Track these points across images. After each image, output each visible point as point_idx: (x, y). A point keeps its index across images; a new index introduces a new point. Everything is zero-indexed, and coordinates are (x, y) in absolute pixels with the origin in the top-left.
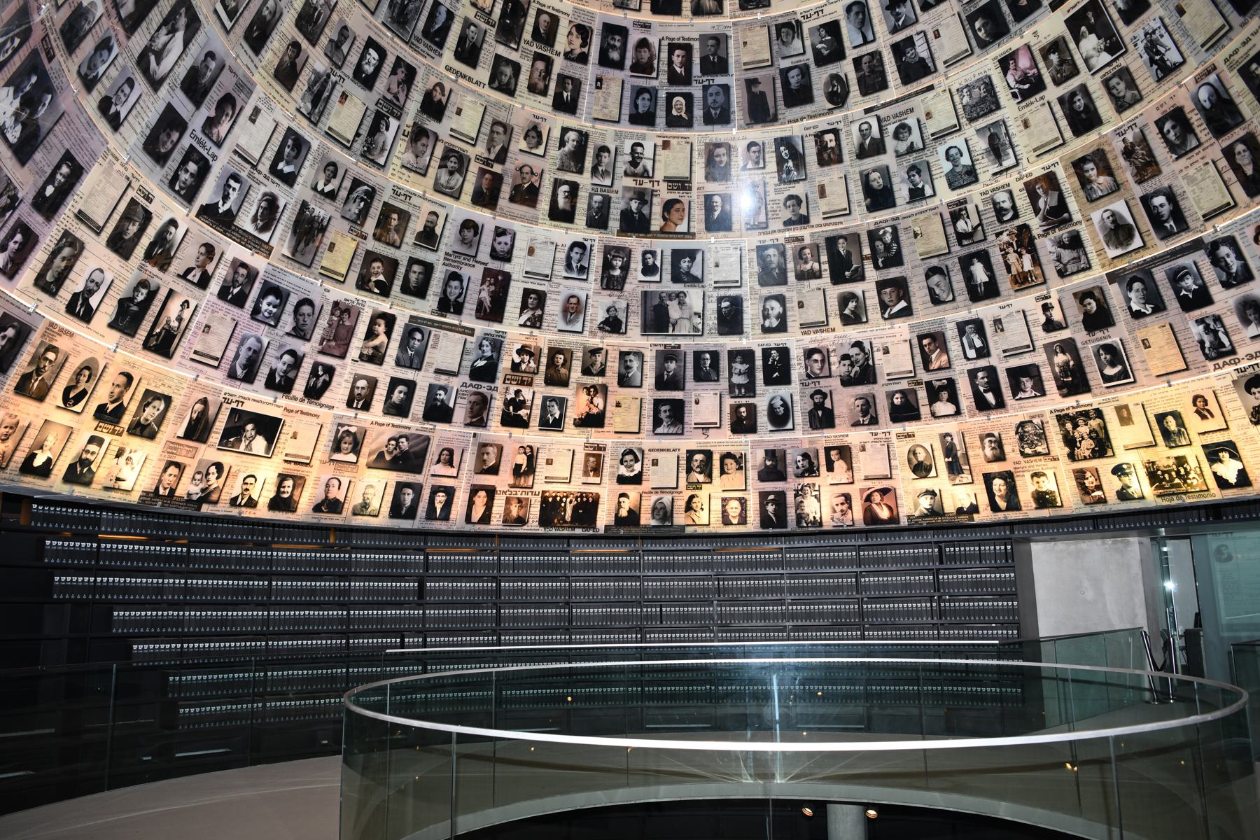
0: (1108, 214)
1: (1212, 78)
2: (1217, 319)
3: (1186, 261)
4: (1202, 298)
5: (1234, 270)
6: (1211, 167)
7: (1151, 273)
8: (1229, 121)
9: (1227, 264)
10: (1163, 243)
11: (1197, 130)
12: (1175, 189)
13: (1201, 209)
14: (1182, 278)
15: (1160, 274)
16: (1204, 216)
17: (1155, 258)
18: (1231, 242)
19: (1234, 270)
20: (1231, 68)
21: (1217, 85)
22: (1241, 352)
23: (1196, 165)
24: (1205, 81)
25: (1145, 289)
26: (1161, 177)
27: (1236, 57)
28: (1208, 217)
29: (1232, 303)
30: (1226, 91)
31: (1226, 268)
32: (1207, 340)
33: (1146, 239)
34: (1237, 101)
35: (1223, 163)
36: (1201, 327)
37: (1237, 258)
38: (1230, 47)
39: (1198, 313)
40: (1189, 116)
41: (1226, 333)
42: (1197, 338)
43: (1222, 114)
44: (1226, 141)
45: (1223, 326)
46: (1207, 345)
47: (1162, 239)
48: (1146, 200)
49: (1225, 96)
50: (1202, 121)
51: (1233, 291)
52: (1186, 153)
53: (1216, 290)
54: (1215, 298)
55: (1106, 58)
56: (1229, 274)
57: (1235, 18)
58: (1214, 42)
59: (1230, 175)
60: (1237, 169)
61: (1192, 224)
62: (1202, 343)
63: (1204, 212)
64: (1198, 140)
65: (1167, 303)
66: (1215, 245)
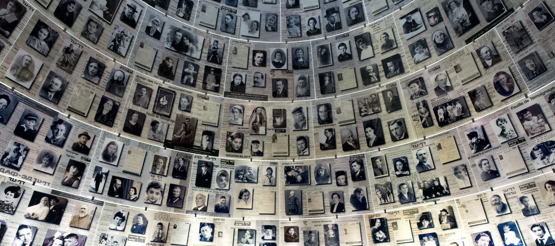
0: (29, 59)
1: (127, 74)
2: (27, 150)
3: (41, 115)
4: (31, 136)
5: (57, 138)
6: (92, 97)
7: (17, 103)
8: (117, 91)
9: (57, 133)
10: (39, 97)
11: (102, 80)
12: (69, 85)
13: (71, 104)
14: (30, 119)
15: (21, 108)
16: (69, 107)
17: (28, 99)
18: (69, 127)
19: (57, 138)
20: (136, 80)
21: (126, 78)
22: (22, 172)
23: (88, 89)
24: (124, 72)
25: (6, 107)
26: (69, 75)
27: (142, 80)
28: (70, 109)
29: (41, 149)
30: (127, 83)
31: (55, 134)
32: (12, 154)
33: (33, 88)
34: (127, 90)
35: (99, 100)
36: (15, 147)
37: (64, 135)
38: (144, 74)
39: (20, 140)
40: (105, 72)
41: (24, 159)
42: (6, 150)
43: (117, 85)
44: (108, 95)
45: (26, 155)
46: (8, 157)
47: (41, 96)
48: (52, 75)
49: (125, 84)
50: (108, 80)
51: (48, 145)
52: (89, 81)
53: (40, 139)
54: (36, 140)
55: (101, 14)
56: (54, 137)
57: (155, 71)
58: (140, 67)
59: (96, 106)
60: (101, 107)
61: (60, 104)
62: (7, 154)
63: (71, 106)
64: (99, 82)
65: (10, 122)
66: (61, 122)
